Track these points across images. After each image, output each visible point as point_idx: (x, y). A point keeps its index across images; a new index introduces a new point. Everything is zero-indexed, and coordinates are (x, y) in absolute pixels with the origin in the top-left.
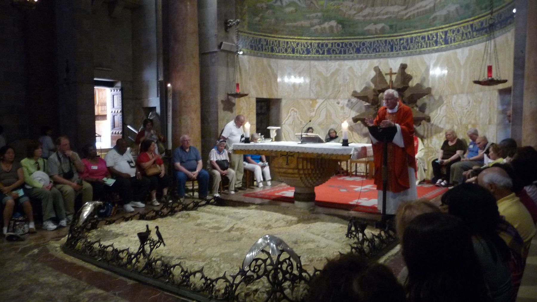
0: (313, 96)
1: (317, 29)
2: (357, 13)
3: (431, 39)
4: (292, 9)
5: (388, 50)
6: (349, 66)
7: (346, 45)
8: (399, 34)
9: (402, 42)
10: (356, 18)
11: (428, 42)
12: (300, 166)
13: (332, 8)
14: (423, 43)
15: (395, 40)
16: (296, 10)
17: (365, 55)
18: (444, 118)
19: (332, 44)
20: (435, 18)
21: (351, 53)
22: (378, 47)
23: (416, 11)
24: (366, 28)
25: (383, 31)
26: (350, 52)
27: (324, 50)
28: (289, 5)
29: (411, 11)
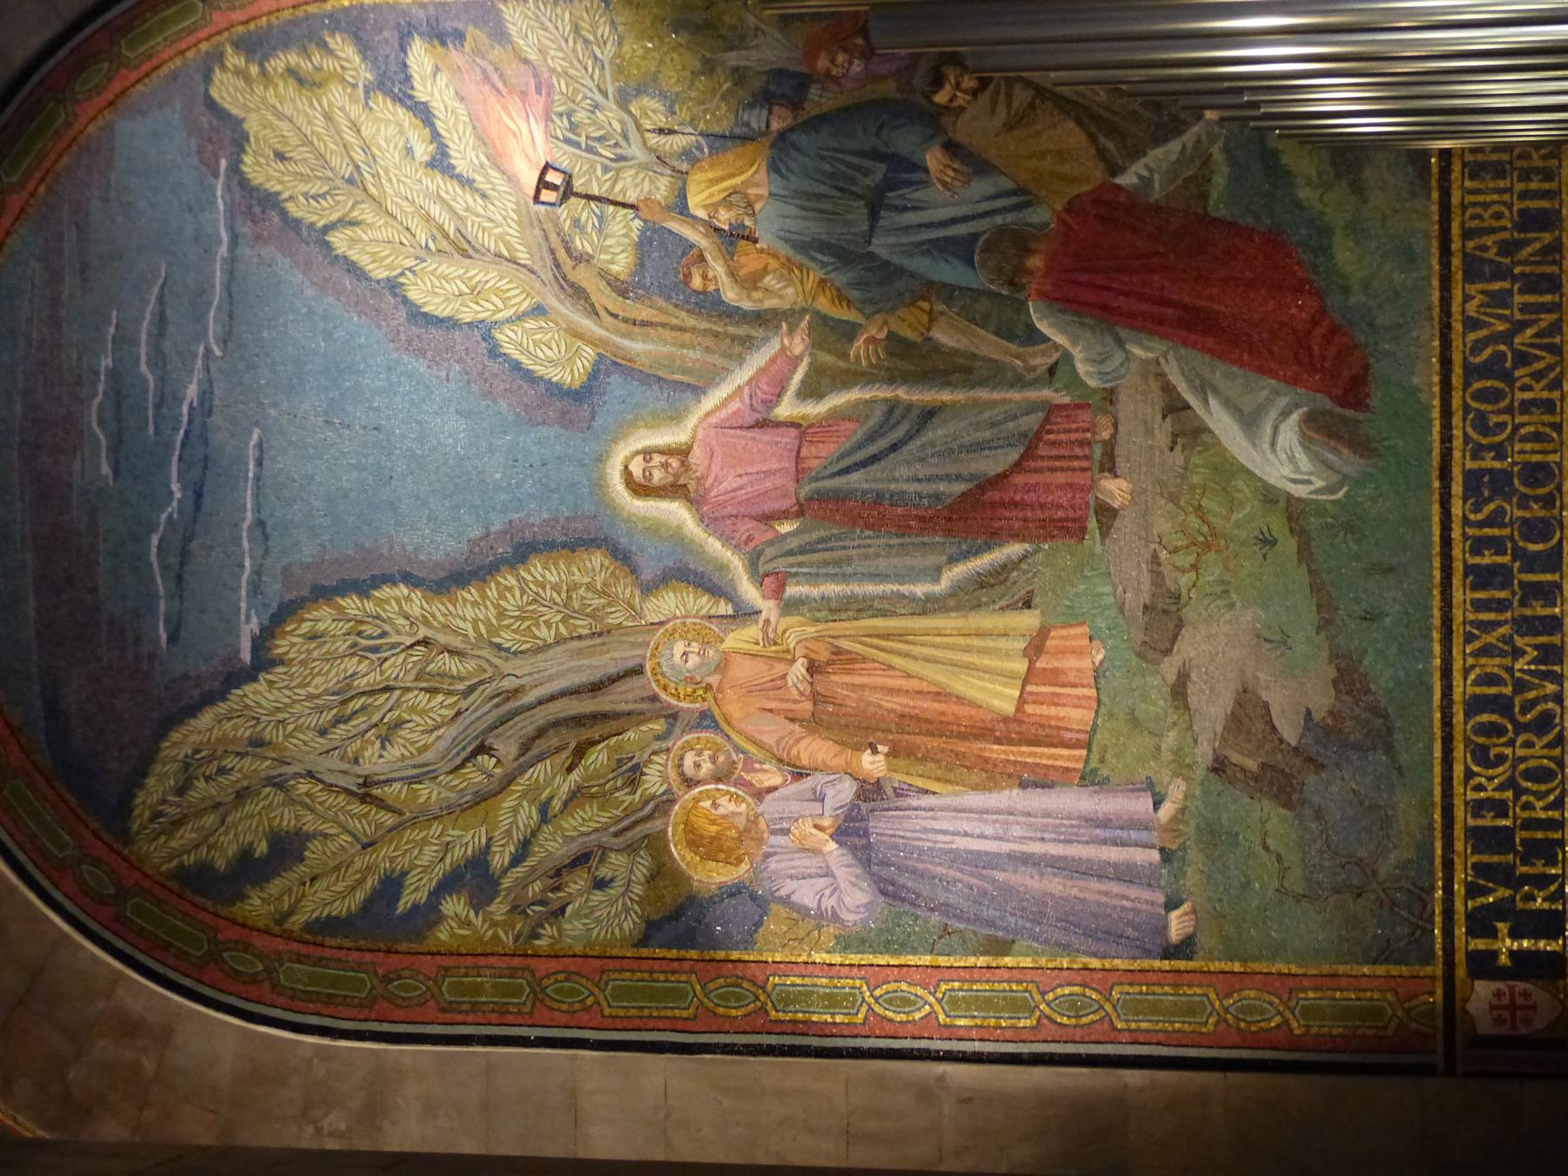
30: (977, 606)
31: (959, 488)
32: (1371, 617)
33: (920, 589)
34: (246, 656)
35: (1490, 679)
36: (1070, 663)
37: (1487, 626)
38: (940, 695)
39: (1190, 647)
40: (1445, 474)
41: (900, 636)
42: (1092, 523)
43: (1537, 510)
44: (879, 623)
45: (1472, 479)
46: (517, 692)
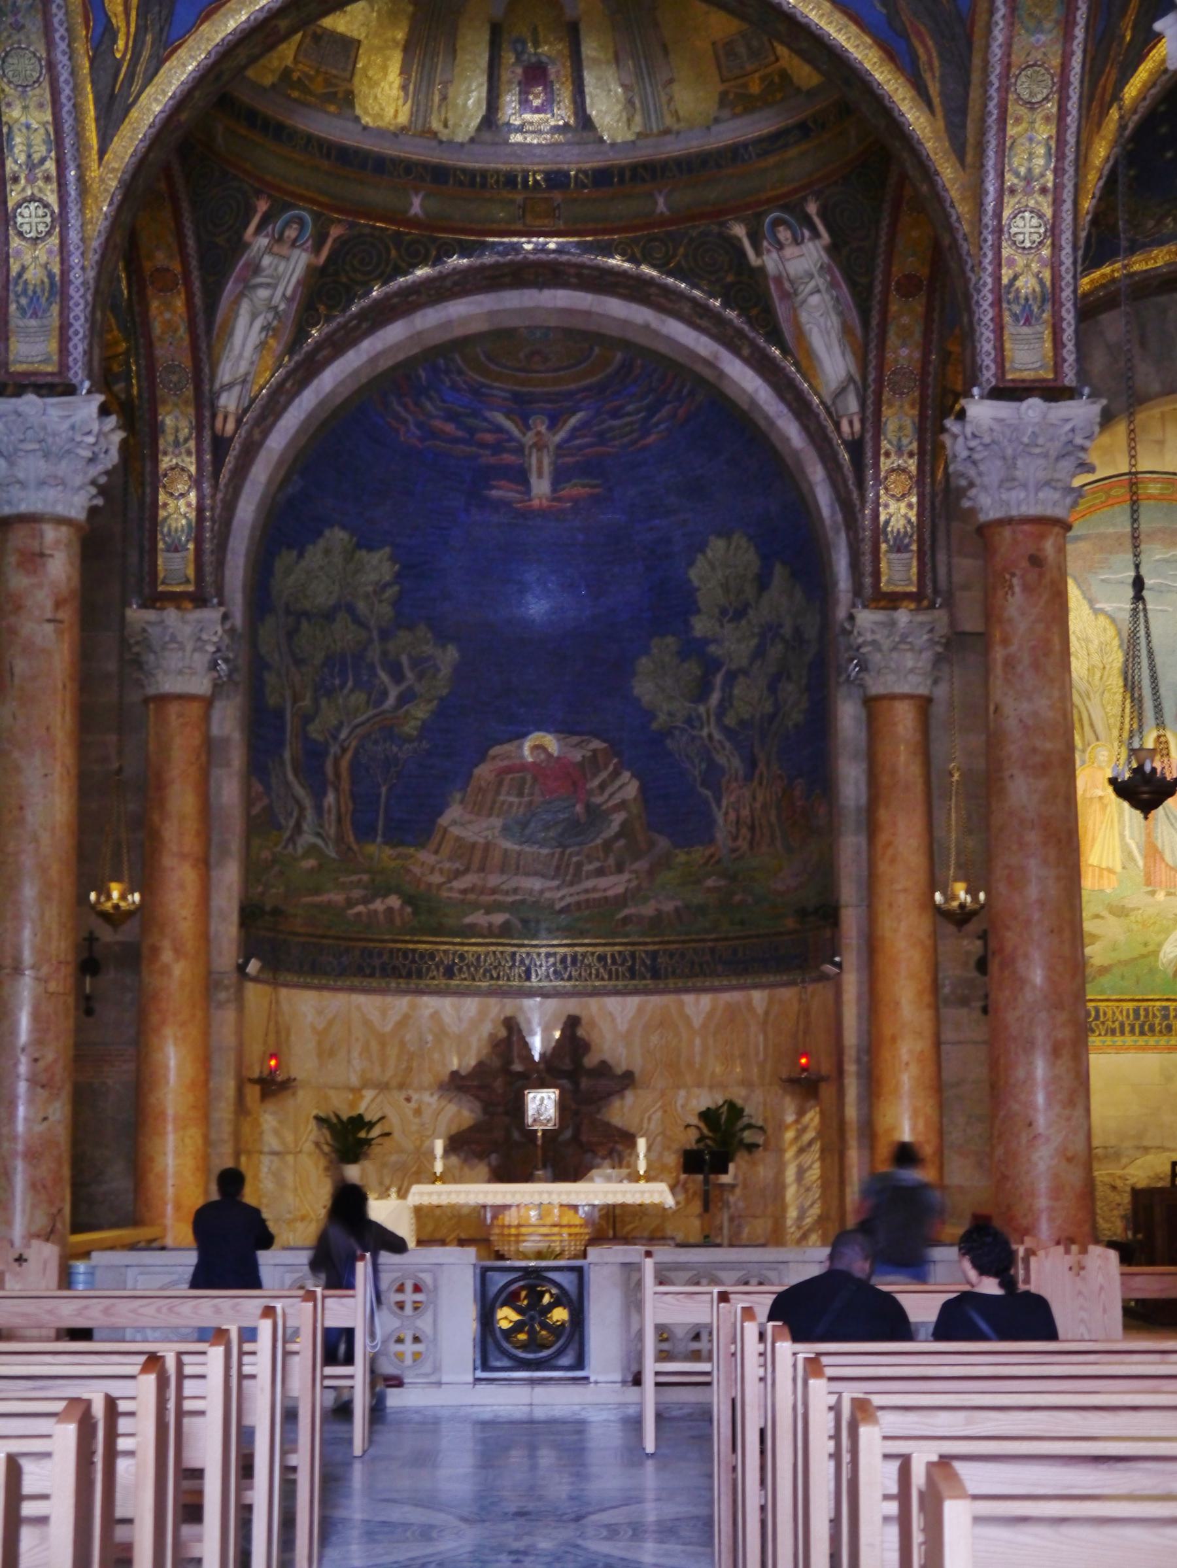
0: (354, 1080)
1: (359, 914)
2: (444, 883)
3: (619, 961)
4: (310, 863)
5: (520, 976)
6: (431, 1010)
7: (422, 956)
8: (545, 942)
9: (552, 960)
10: (445, 894)
11: (614, 968)
12: (565, 1221)
13: (393, 864)
14: (602, 970)
15: (535, 956)
16: (320, 866)
17: (466, 983)
18: (659, 1138)
19: (391, 951)
20: (626, 920)
21: (433, 978)
22: (495, 968)
23: (583, 897)
24: (468, 920)
25: (505, 930)
26: (431, 975)
27: (374, 968)
28: (307, 854)
29: (571, 895)
30: (1123, 852)
31: (1159, 845)
32: (1123, 977)
33: (1127, 833)
34: (1098, 606)
35: (1105, 1014)
36: (1105, 881)
37: (1121, 1012)
38: (1094, 839)
39: (1112, 920)
40: (1168, 1000)
41: (1112, 827)
42: (1150, 889)
43: (1158, 1029)
44: (1116, 819)
45: (1166, 1008)
46: (1089, 698)
